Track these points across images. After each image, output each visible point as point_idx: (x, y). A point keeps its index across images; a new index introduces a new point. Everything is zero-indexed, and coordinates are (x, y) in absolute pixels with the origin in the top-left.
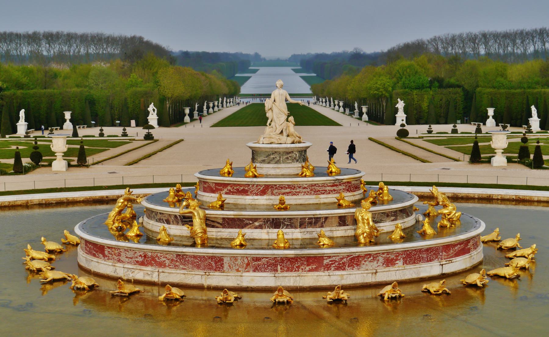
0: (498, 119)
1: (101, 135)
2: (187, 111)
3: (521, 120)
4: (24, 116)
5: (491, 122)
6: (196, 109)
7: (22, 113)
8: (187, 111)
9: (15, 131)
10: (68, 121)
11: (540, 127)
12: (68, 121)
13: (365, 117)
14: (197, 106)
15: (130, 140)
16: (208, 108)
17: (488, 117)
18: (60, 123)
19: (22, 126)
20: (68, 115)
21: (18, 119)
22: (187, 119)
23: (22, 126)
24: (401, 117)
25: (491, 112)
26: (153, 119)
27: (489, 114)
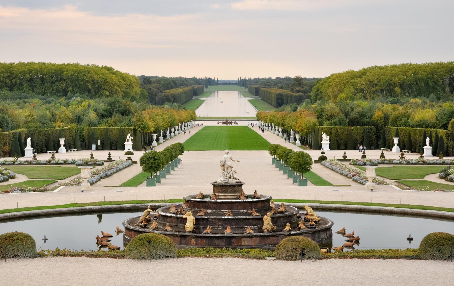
0: (403, 147)
2: (155, 137)
4: (30, 143)
5: (396, 148)
6: (162, 135)
7: (29, 141)
8: (155, 137)
9: (23, 155)
10: (62, 146)
12: (62, 146)
13: (298, 142)
14: (162, 132)
16: (170, 132)
17: (394, 145)
18: (56, 147)
19: (29, 150)
20: (62, 141)
23: (29, 150)
25: (396, 141)
26: (129, 145)
27: (394, 142)
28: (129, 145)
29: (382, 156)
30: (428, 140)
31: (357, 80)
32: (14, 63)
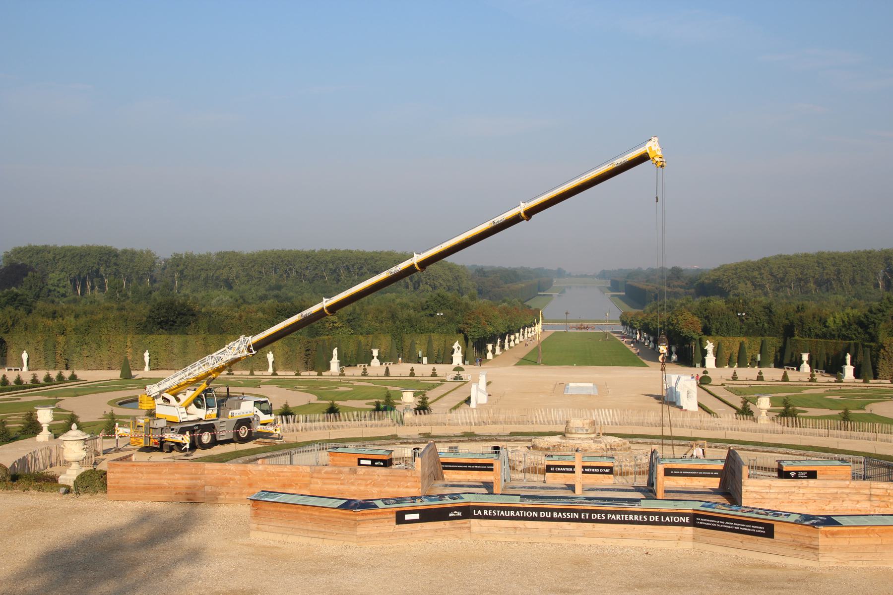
1: (412, 374)
3: (834, 368)
5: (806, 368)
7: (335, 352)
8: (490, 347)
11: (855, 375)
13: (674, 357)
15: (442, 381)
16: (509, 341)
18: (368, 359)
19: (335, 364)
21: (331, 357)
22: (490, 356)
23: (335, 364)
24: (710, 360)
25: (805, 357)
26: (457, 357)
28: (457, 357)
29: (785, 378)
30: (848, 357)
31: (756, 274)
32: (314, 251)
